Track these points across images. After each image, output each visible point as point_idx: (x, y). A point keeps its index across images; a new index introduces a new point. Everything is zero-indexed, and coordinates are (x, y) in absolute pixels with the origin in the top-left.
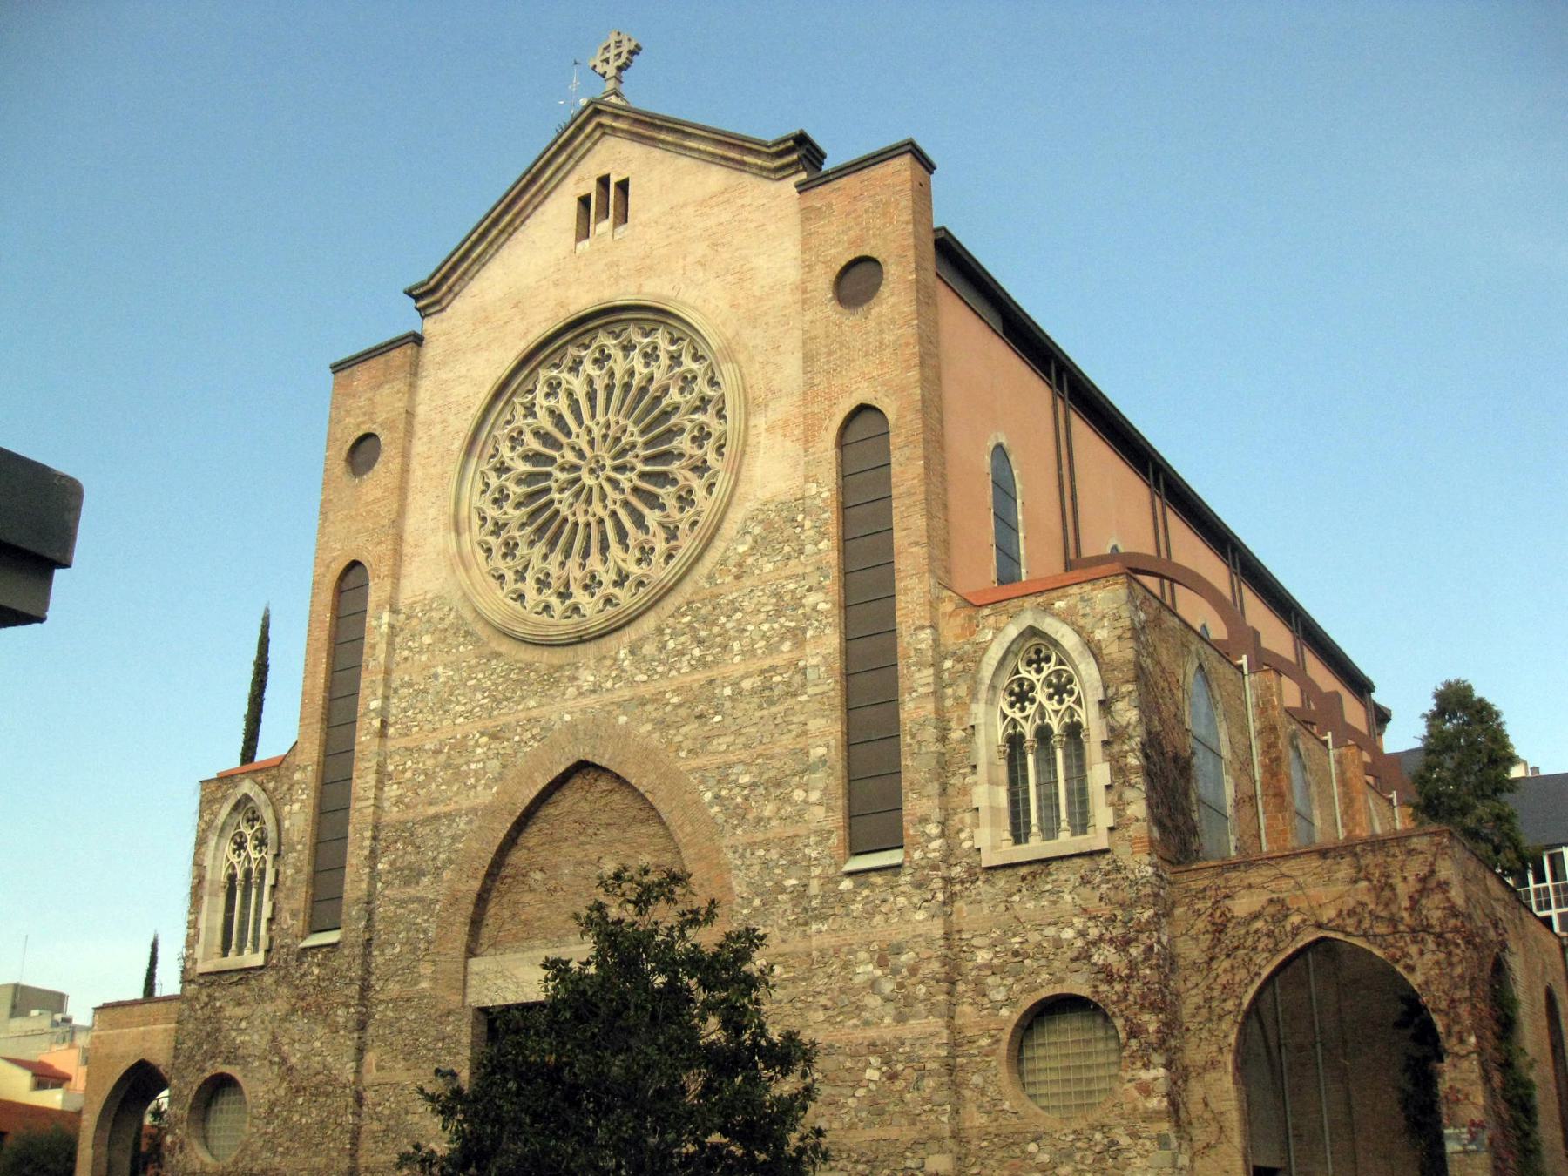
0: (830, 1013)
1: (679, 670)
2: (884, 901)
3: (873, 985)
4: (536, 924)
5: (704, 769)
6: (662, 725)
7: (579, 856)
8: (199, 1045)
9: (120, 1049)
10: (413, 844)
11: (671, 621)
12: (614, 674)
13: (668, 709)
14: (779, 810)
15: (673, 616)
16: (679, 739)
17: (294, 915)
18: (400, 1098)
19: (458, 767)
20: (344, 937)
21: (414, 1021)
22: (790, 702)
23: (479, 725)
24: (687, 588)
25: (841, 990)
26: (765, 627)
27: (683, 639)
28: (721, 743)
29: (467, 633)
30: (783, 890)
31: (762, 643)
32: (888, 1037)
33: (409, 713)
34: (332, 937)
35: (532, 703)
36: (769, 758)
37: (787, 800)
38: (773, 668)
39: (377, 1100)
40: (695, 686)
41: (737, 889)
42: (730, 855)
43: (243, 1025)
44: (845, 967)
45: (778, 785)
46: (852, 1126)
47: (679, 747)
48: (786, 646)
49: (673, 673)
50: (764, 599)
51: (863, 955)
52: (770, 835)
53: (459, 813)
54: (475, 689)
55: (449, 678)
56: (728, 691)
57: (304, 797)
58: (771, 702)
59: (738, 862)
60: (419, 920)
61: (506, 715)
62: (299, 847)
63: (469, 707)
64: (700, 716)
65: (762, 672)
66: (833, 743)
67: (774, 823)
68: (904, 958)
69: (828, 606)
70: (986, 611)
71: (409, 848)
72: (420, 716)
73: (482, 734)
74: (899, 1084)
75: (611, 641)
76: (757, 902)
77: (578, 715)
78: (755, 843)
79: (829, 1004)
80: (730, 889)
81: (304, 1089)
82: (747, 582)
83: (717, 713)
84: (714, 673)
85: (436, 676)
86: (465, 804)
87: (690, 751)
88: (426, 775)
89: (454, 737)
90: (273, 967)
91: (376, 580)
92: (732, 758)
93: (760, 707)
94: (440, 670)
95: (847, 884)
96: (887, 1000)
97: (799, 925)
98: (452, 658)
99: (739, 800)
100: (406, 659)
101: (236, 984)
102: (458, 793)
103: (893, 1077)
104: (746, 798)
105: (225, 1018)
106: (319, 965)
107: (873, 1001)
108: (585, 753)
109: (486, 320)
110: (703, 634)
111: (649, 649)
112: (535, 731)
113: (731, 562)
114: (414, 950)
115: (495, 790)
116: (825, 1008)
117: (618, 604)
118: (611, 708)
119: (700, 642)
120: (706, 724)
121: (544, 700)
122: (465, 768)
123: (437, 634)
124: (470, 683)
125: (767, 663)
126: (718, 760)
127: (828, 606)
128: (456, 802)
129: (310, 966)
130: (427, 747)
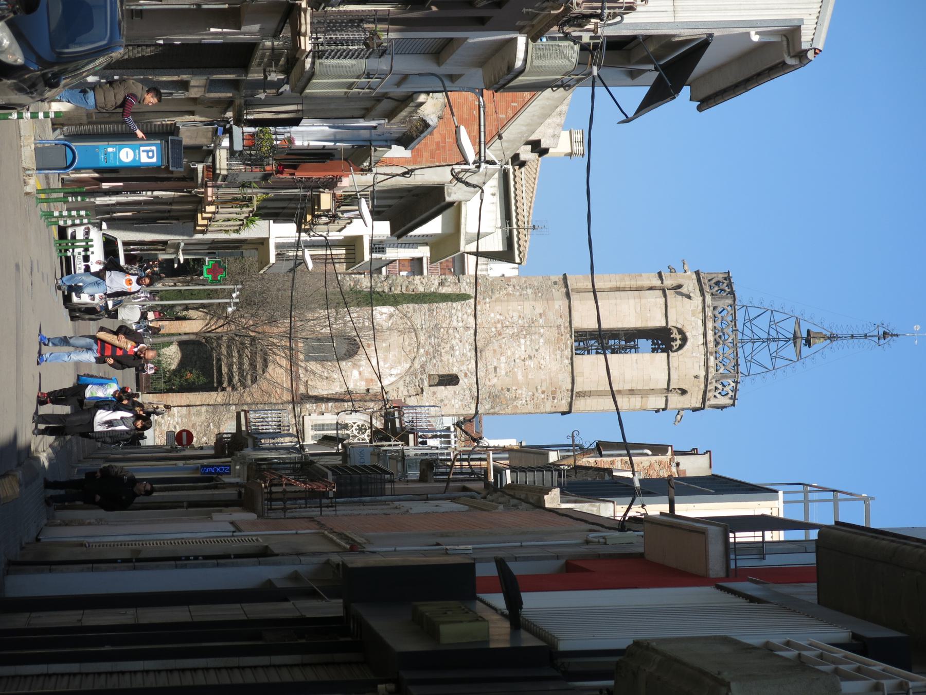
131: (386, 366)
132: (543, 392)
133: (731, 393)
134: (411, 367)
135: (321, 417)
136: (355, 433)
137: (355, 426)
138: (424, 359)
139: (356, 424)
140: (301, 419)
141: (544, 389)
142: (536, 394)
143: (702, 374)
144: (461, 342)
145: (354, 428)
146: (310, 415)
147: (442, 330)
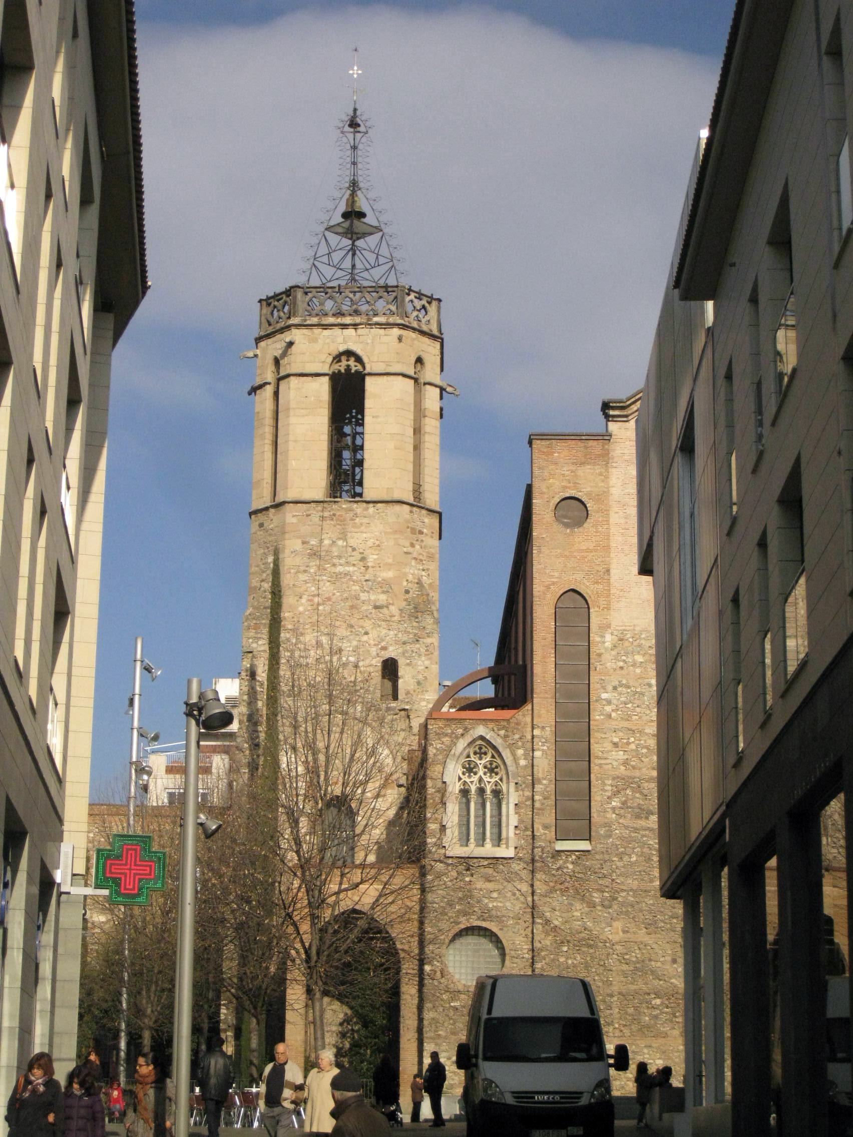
8: (451, 904)
10: (641, 793)
17: (546, 827)
21: (653, 905)
33: (629, 706)
34: (584, 845)
39: (625, 951)
43: (495, 895)
60: (651, 842)
71: (638, 795)
72: (638, 710)
81: (568, 942)
88: (648, 749)
90: (520, 859)
100: (622, 668)
105: (476, 889)
106: (573, 863)
123: (647, 657)
129: (565, 863)
137: (465, 778)
139: (462, 776)
140: (450, 861)
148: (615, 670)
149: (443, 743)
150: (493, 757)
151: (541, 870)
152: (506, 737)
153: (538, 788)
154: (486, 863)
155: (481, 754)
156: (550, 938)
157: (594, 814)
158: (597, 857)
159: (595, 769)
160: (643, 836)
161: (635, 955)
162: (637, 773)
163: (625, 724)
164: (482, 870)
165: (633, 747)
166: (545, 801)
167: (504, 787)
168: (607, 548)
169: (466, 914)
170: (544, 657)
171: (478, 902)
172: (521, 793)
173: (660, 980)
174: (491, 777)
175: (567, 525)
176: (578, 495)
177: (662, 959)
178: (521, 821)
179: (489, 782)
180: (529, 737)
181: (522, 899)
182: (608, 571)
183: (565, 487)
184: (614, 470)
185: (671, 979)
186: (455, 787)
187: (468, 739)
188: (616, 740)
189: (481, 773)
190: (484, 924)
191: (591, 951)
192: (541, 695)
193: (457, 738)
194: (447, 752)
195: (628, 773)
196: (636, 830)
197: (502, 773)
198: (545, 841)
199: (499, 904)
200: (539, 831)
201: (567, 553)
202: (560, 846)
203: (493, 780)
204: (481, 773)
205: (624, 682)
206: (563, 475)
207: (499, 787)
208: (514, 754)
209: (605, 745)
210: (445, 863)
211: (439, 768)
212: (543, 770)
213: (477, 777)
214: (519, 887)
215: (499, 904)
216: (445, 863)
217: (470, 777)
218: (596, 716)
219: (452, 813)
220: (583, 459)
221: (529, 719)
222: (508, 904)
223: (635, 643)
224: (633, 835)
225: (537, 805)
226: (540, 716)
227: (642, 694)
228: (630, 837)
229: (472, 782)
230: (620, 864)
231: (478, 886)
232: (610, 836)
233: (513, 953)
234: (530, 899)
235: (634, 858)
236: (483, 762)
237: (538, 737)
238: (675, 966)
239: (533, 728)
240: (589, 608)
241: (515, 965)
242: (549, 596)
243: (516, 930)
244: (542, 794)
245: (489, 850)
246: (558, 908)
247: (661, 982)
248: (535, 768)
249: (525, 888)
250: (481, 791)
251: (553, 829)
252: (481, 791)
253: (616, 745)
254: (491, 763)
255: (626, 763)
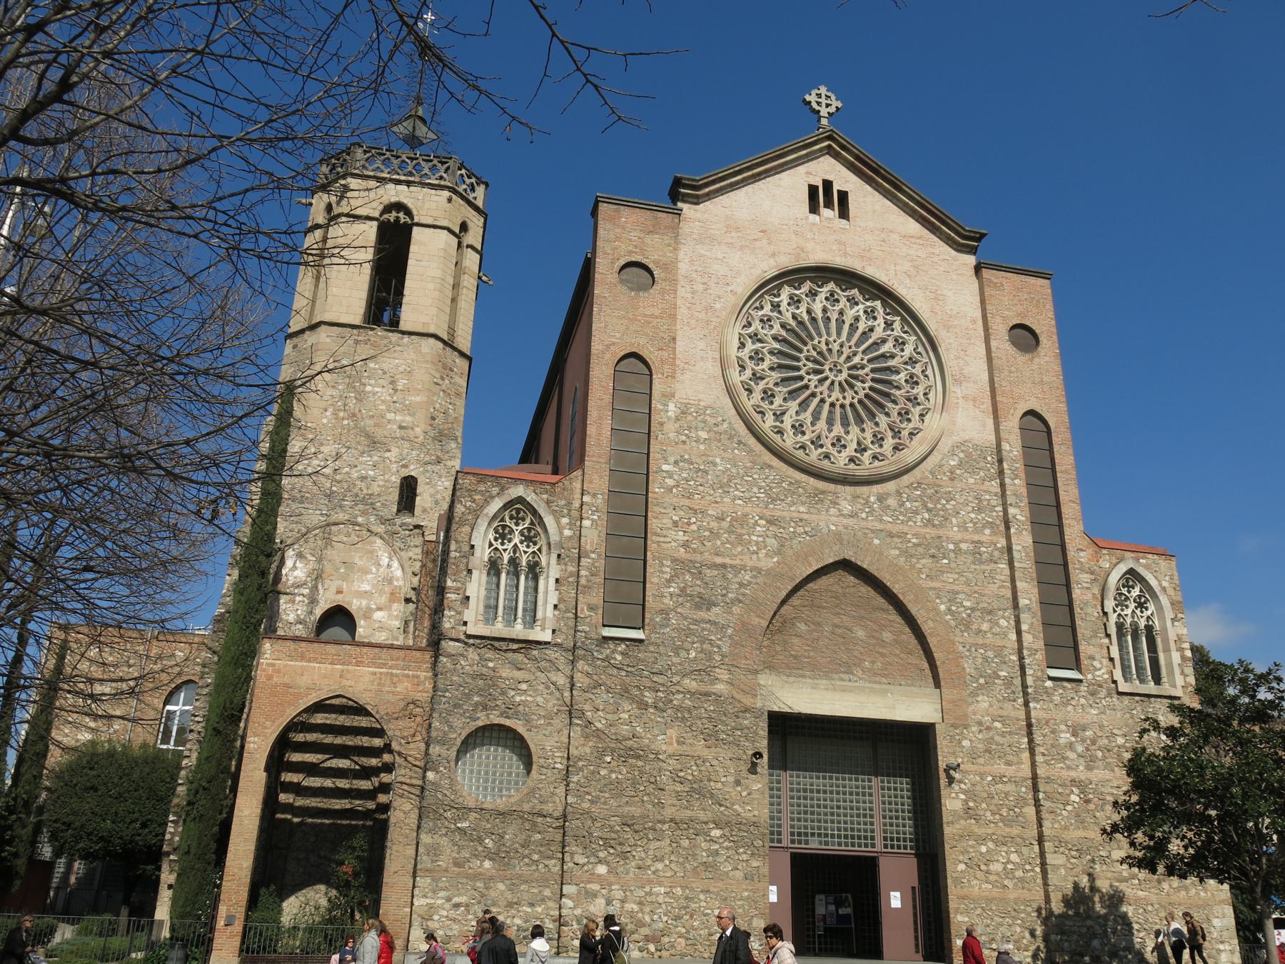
0: (1046, 758)
1: (915, 522)
2: (1073, 698)
3: (1071, 746)
4: (652, 648)
5: (940, 590)
6: (906, 553)
7: (836, 621)
8: (468, 696)
9: (304, 681)
11: (907, 490)
12: (867, 510)
13: (909, 545)
14: (991, 628)
15: (907, 487)
16: (919, 566)
17: (591, 608)
18: (702, 768)
19: (741, 535)
20: (648, 637)
22: (993, 566)
23: (758, 510)
24: (916, 472)
25: (1053, 746)
26: (973, 516)
27: (916, 504)
28: (950, 577)
29: (740, 443)
30: (998, 677)
31: (971, 525)
32: (1083, 778)
33: (692, 483)
35: (802, 509)
36: (981, 595)
37: (997, 624)
38: (979, 542)
39: (679, 767)
40: (927, 536)
41: (968, 670)
42: (961, 648)
43: (524, 686)
44: (1053, 732)
45: (990, 613)
46: (1066, 828)
47: (920, 571)
48: (987, 531)
49: (910, 523)
50: (970, 499)
51: (1063, 727)
52: (987, 642)
53: (743, 568)
54: (751, 484)
55: (727, 469)
56: (951, 547)
57: (595, 517)
58: (981, 563)
59: (968, 654)
60: (713, 638)
61: (780, 510)
62: (593, 556)
63: (747, 494)
64: (933, 556)
65: (973, 542)
66: (1034, 599)
67: (989, 635)
68: (1087, 733)
69: (1023, 519)
70: (1105, 551)
72: (701, 488)
73: (761, 518)
74: (1092, 806)
75: (864, 490)
76: (982, 681)
77: (840, 528)
78: (977, 644)
79: (1046, 752)
80: (964, 669)
82: (959, 485)
83: (944, 558)
84: (941, 532)
85: (715, 464)
86: (750, 564)
87: (927, 576)
88: (711, 532)
89: (736, 513)
90: (556, 645)
91: (660, 376)
92: (956, 588)
93: (974, 563)
94: (718, 460)
95: (1049, 684)
96: (1080, 756)
97: (1009, 700)
98: (727, 455)
99: (964, 615)
100: (684, 442)
101: (514, 651)
102: (741, 553)
103: (1088, 801)
104: (969, 616)
106: (622, 654)
107: (1072, 755)
108: (849, 554)
109: (737, 229)
110: (930, 505)
111: (892, 502)
112: (807, 529)
113: (946, 469)
114: (710, 659)
115: (775, 560)
116: (1043, 754)
117: (833, 463)
118: (867, 531)
119: (929, 510)
120: (937, 562)
121: (812, 510)
122: (746, 537)
123: (712, 434)
124: (746, 478)
125: (976, 538)
126: (949, 587)
127: (1023, 519)
128: (742, 560)
129: (613, 652)
130: (709, 512)
131: (374, 570)
132: (443, 379)
133: (473, 180)
134: (381, 538)
135: (472, 602)
136: (509, 546)
137: (497, 545)
138: (372, 519)
139: (493, 542)
140: (471, 641)
141: (438, 375)
142: (444, 387)
143: (446, 194)
144: (356, 466)
145: (500, 547)
146: (465, 623)
147: (334, 489)
148: (677, 443)
149: (474, 501)
150: (532, 523)
151: (584, 658)
152: (548, 502)
153: (584, 561)
154: (515, 646)
155: (517, 519)
156: (591, 744)
157: (649, 598)
158: (652, 648)
159: (652, 546)
160: (704, 629)
161: (692, 772)
162: (698, 558)
163: (687, 502)
164: (510, 655)
165: (694, 527)
166: (593, 578)
167: (544, 559)
168: (673, 317)
169: (485, 708)
170: (600, 418)
171: (503, 693)
172: (564, 567)
173: (721, 805)
174: (528, 546)
175: (631, 289)
176: (644, 261)
177: (723, 779)
178: (560, 600)
179: (525, 552)
180: (577, 504)
181: (557, 694)
182: (674, 339)
183: (630, 252)
184: (682, 246)
185: (734, 804)
186: (483, 554)
187: (506, 499)
188: (675, 518)
189: (516, 540)
190: (508, 722)
191: (640, 763)
192: (594, 459)
193: (493, 497)
194: (477, 513)
195: (688, 556)
196: (696, 622)
197: (542, 542)
198: (589, 625)
199: (529, 698)
200: (584, 612)
201: (630, 315)
202: (608, 632)
203: (530, 550)
204: (516, 540)
205: (686, 457)
206: (630, 240)
207: (537, 559)
208: (558, 522)
209: (664, 521)
210: (466, 643)
211: (466, 529)
212: (592, 542)
213: (512, 544)
214: (554, 679)
215: (529, 698)
216: (466, 643)
217: (503, 544)
218: (655, 489)
219: (477, 586)
220: (651, 229)
221: (577, 485)
222: (539, 699)
223: (699, 418)
224: (691, 627)
225: (583, 581)
226: (591, 482)
227: (706, 472)
228: (689, 629)
229: (505, 550)
230: (675, 660)
231: (504, 675)
232: (667, 625)
233: (542, 761)
234: (567, 694)
235: (693, 654)
236: (520, 528)
237: (587, 504)
238: (739, 789)
239: (582, 495)
240: (651, 375)
241: (543, 777)
242: (608, 356)
243: (547, 733)
244: (589, 569)
245: (519, 630)
246: (601, 707)
247: (722, 809)
248: (583, 539)
249: (561, 680)
250: (514, 562)
251: (600, 611)
252: (514, 562)
253: (675, 524)
254: (529, 529)
255: (686, 545)
